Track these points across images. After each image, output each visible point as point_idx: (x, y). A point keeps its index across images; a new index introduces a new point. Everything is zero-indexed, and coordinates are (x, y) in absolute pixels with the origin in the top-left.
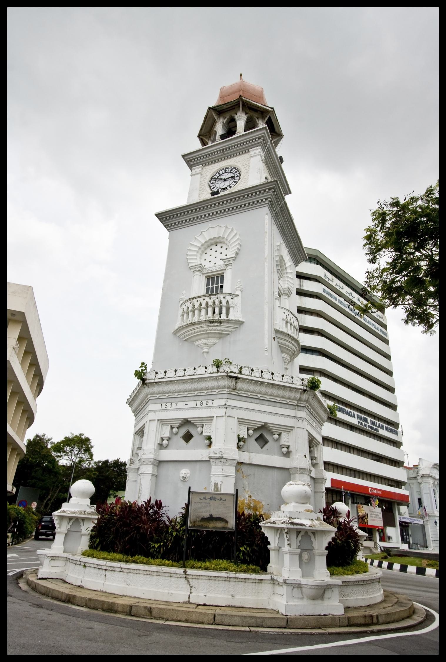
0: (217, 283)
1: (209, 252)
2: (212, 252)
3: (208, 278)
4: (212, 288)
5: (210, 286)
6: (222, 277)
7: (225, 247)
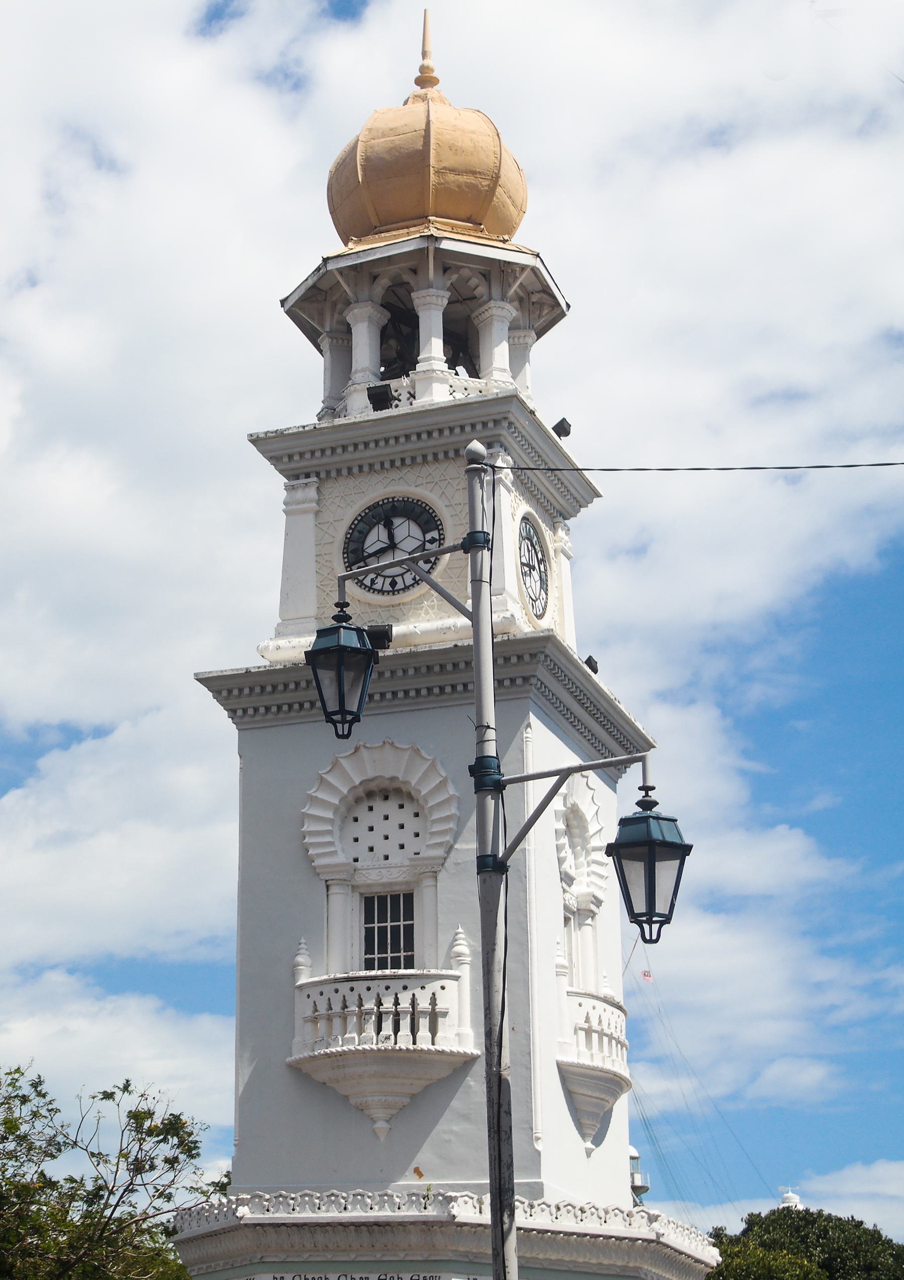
0: (395, 918)
1: (367, 819)
2: (375, 818)
3: (368, 902)
4: (382, 931)
5: (376, 925)
6: (409, 898)
7: (409, 809)
